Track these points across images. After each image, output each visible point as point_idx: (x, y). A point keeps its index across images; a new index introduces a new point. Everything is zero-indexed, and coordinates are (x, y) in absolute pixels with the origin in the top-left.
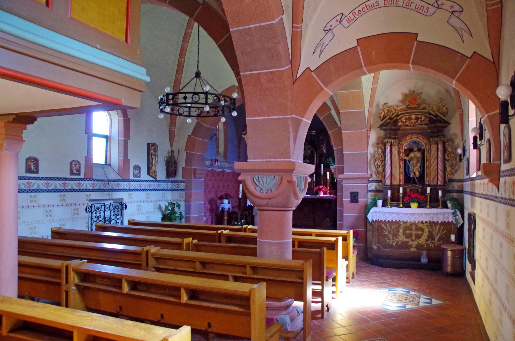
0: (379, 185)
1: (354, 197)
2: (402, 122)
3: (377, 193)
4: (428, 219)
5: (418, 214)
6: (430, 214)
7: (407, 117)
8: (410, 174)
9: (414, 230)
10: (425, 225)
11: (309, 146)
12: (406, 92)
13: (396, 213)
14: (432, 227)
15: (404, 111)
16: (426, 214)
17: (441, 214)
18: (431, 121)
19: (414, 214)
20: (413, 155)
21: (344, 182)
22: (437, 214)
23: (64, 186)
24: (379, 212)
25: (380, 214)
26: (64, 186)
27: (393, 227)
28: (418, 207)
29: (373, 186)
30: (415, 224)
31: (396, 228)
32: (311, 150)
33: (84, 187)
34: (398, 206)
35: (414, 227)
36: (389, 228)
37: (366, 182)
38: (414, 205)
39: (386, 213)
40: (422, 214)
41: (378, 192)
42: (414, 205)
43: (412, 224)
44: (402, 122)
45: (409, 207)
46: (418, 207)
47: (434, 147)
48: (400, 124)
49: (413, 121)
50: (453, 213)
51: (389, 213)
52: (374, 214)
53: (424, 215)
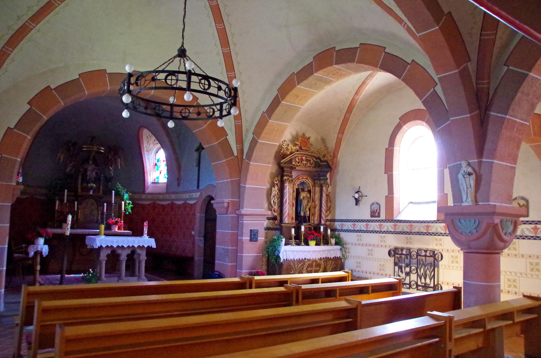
0: (270, 223)
1: (254, 236)
2: (296, 161)
3: (268, 231)
4: (324, 256)
5: (317, 251)
6: (325, 251)
7: (300, 158)
8: (300, 212)
9: (314, 266)
10: (322, 261)
11: (93, 166)
12: (294, 133)
13: (302, 251)
14: (327, 263)
15: (298, 151)
16: (323, 251)
17: (332, 250)
18: (317, 165)
19: (315, 251)
20: (304, 195)
21: (245, 218)
22: (330, 250)
23: (380, 228)
24: (289, 251)
25: (290, 253)
26: (380, 228)
27: (300, 265)
28: (316, 245)
29: (266, 223)
30: (316, 261)
31: (302, 265)
32: (96, 171)
33: (358, 228)
34: (298, 244)
35: (314, 264)
36: (296, 266)
37: (263, 219)
38: (312, 243)
39: (294, 251)
40: (320, 251)
41: (269, 230)
42: (312, 243)
43: (313, 262)
44: (296, 161)
45: (307, 244)
46: (316, 245)
47: (317, 189)
48: (294, 163)
49: (304, 162)
50: (341, 249)
51: (296, 251)
52: (285, 253)
53: (321, 252)
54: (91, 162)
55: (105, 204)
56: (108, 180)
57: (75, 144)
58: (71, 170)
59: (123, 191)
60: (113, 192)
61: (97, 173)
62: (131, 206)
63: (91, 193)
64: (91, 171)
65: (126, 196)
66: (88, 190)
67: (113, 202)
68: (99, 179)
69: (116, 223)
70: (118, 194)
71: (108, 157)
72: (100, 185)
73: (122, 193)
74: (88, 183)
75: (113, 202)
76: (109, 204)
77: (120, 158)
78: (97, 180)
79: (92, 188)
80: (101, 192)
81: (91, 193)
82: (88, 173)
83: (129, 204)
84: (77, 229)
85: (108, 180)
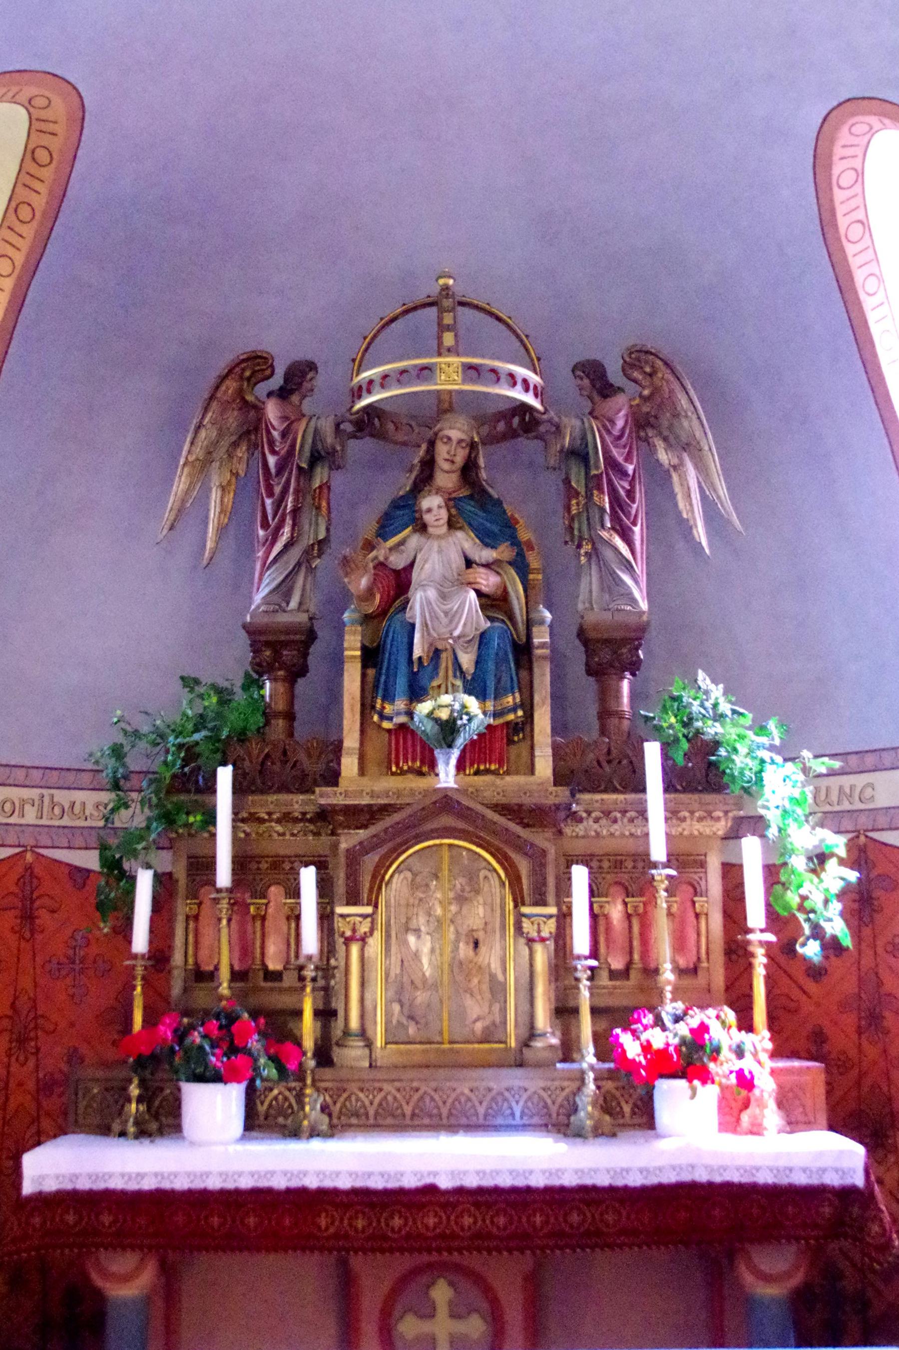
32: (488, 581)
54: (432, 504)
55: (580, 875)
56: (610, 652)
57: (299, 376)
58: (284, 590)
59: (746, 747)
60: (652, 752)
61: (494, 603)
62: (839, 876)
63: (447, 775)
64: (447, 589)
65: (781, 788)
66: (413, 750)
67: (658, 851)
68: (523, 652)
69: (690, 1062)
70: (700, 773)
71: (580, 454)
72: (528, 707)
73: (741, 763)
74: (417, 693)
75: (658, 851)
76: (622, 872)
77: (690, 447)
78: (508, 658)
79: (448, 730)
80: (544, 766)
81: (447, 775)
82: (421, 600)
83: (820, 859)
84: (332, 1132)
85: (610, 652)
